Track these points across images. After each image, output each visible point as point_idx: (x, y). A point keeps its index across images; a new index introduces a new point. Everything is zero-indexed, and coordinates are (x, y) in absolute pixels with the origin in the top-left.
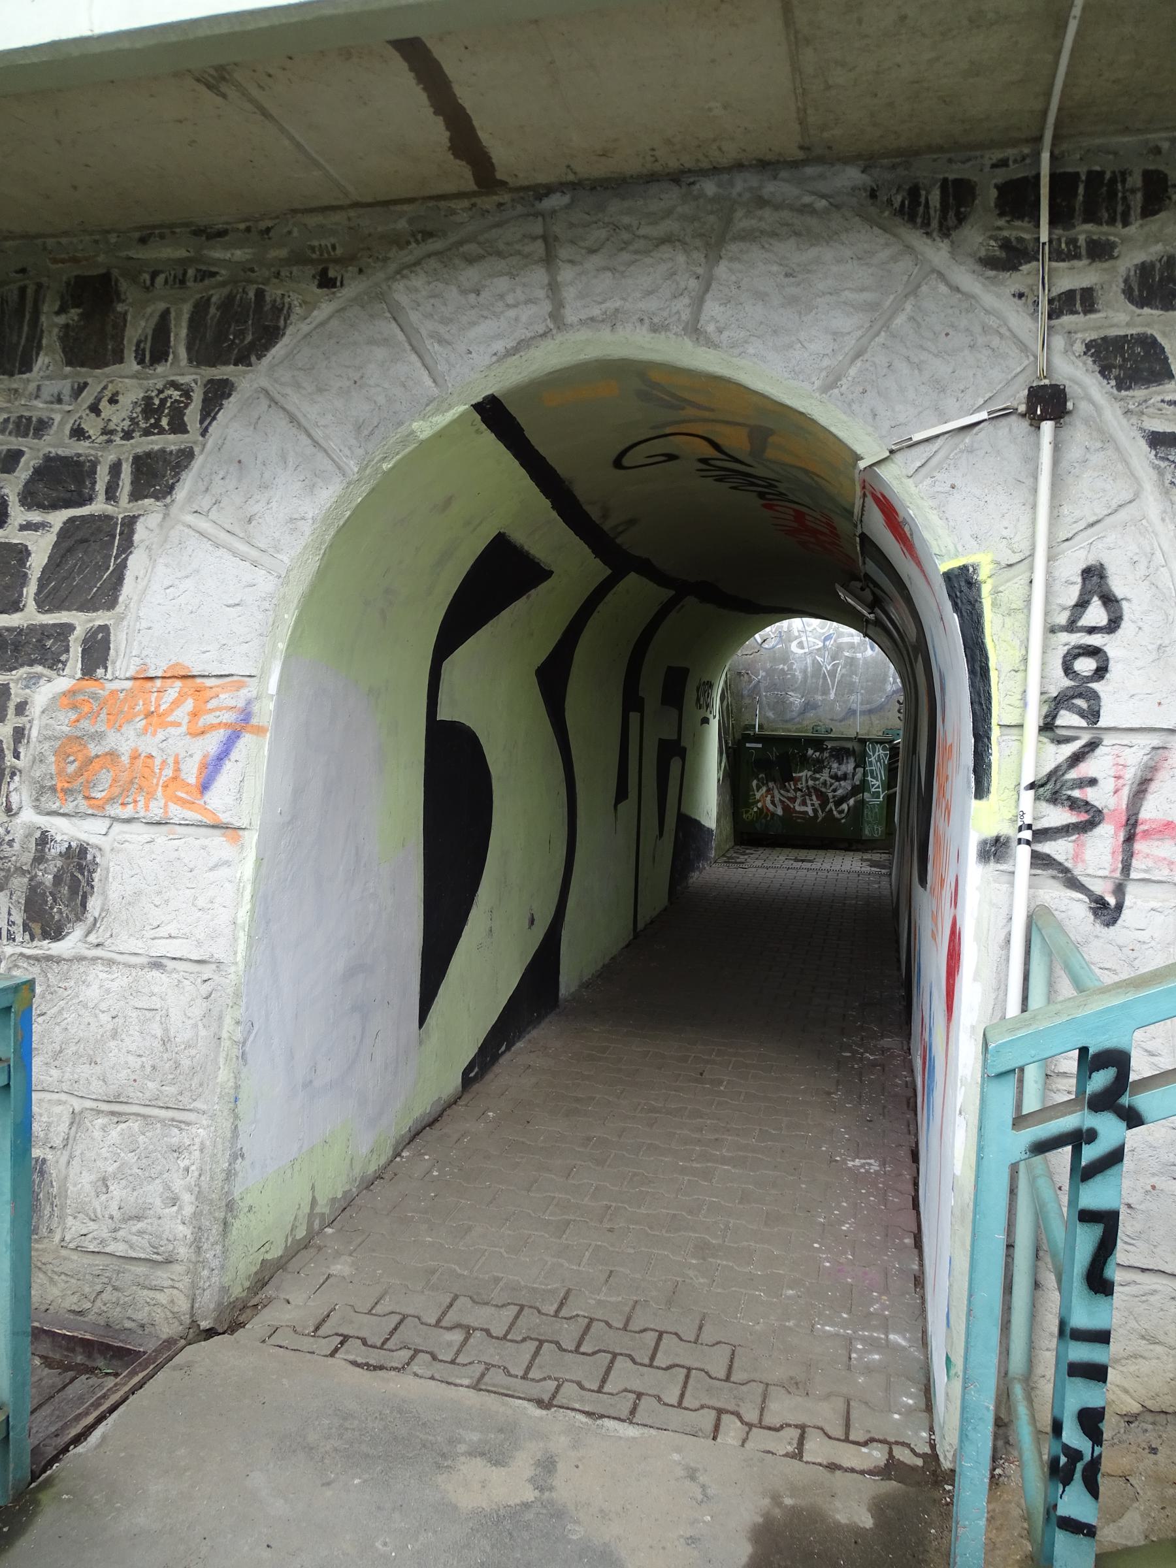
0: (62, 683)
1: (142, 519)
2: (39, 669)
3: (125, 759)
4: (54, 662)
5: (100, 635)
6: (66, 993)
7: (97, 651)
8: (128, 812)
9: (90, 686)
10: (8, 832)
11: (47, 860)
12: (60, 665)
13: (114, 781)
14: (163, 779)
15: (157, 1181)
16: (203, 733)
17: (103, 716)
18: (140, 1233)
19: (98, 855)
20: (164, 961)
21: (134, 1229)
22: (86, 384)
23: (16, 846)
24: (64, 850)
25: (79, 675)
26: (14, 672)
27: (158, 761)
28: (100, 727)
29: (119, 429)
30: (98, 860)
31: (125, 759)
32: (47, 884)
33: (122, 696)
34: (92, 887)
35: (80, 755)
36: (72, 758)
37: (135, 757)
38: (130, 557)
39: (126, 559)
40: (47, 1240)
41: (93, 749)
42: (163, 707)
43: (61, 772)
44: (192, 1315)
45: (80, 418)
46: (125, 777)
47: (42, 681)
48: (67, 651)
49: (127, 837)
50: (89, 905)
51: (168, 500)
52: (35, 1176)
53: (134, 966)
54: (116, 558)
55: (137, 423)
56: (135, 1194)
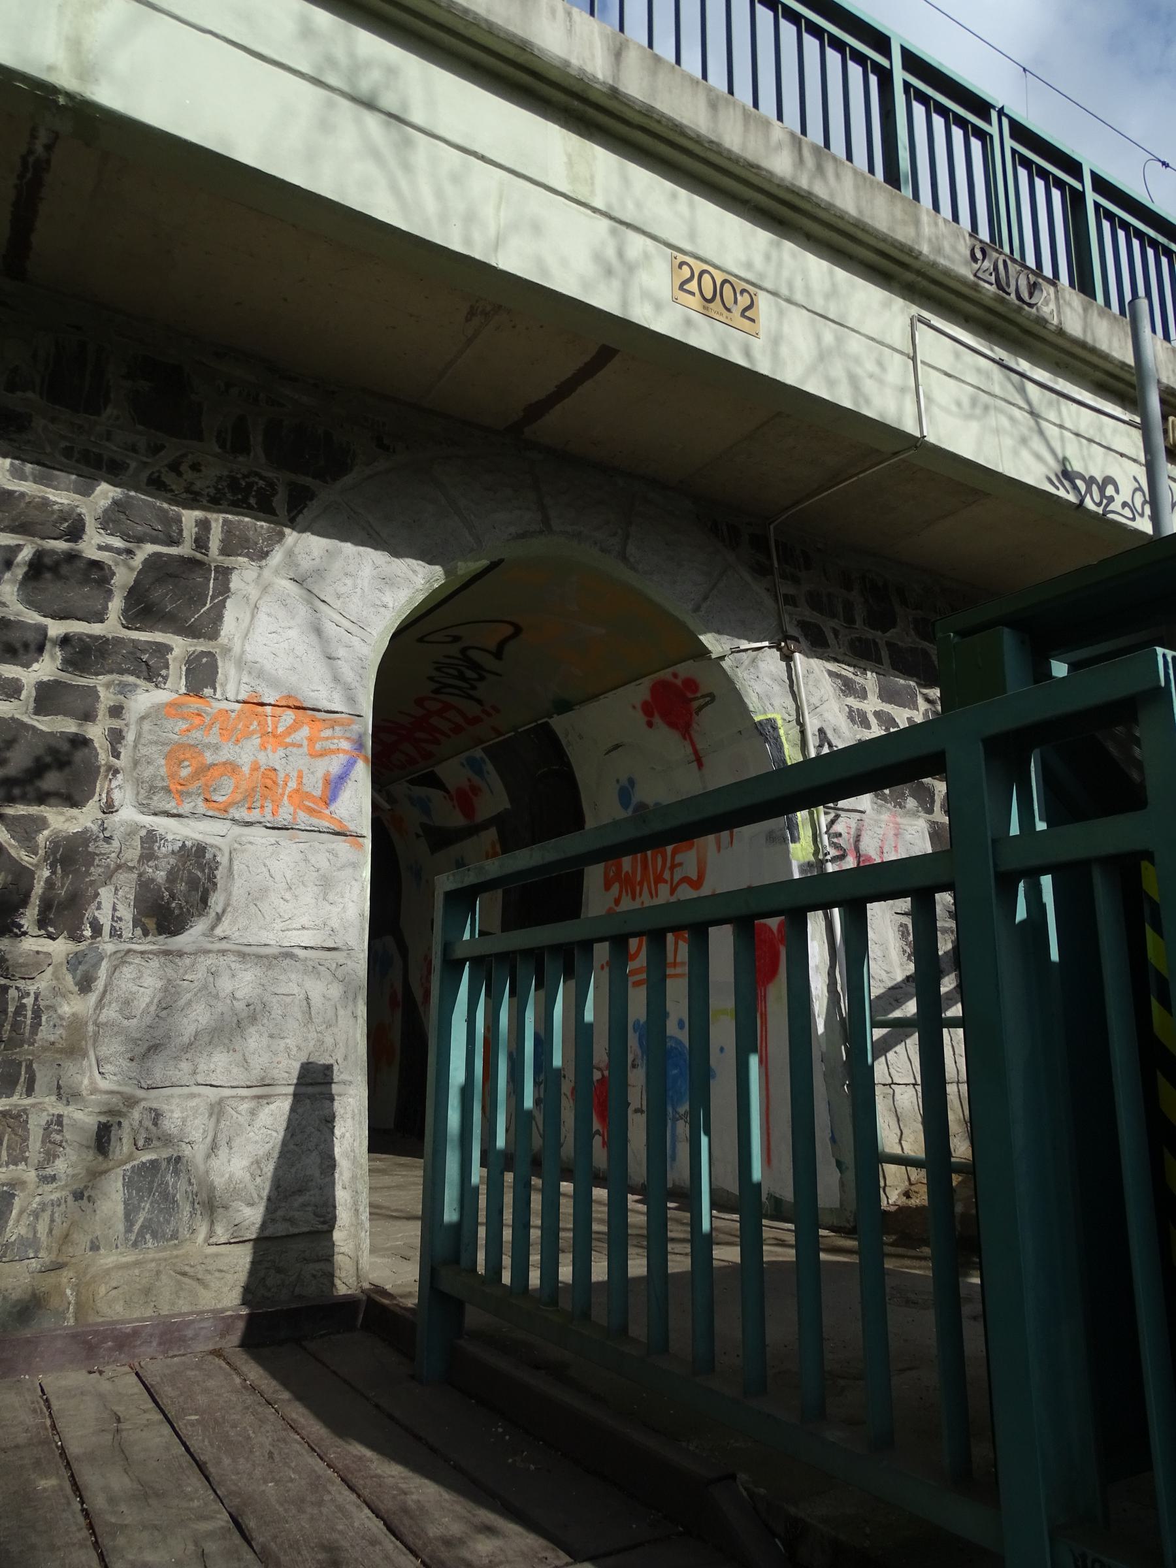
0: (161, 696)
1: (236, 572)
2: (131, 679)
3: (246, 769)
4: (152, 674)
5: (204, 660)
6: (192, 985)
7: (201, 675)
8: (255, 815)
9: (194, 703)
10: (105, 829)
11: (157, 858)
12: (160, 679)
13: (237, 787)
14: (288, 790)
15: (314, 1154)
16: (321, 755)
17: (215, 729)
18: (304, 1205)
19: (218, 853)
20: (297, 951)
21: (296, 1205)
22: (163, 447)
23: (116, 844)
24: (176, 848)
25: (183, 690)
26: (100, 677)
27: (281, 775)
28: (213, 738)
29: (205, 493)
30: (218, 859)
31: (246, 769)
32: (159, 880)
33: (233, 715)
34: (215, 884)
35: (194, 762)
36: (186, 763)
37: (255, 767)
38: (228, 601)
39: (224, 601)
40: (188, 1243)
41: (209, 757)
42: (280, 730)
43: (172, 776)
44: (358, 1277)
45: (159, 471)
46: (244, 785)
47: (139, 691)
48: (167, 667)
49: (251, 839)
50: (212, 901)
51: (263, 563)
52: (168, 1178)
53: (267, 957)
54: (213, 598)
55: (224, 494)
56: (293, 1170)
